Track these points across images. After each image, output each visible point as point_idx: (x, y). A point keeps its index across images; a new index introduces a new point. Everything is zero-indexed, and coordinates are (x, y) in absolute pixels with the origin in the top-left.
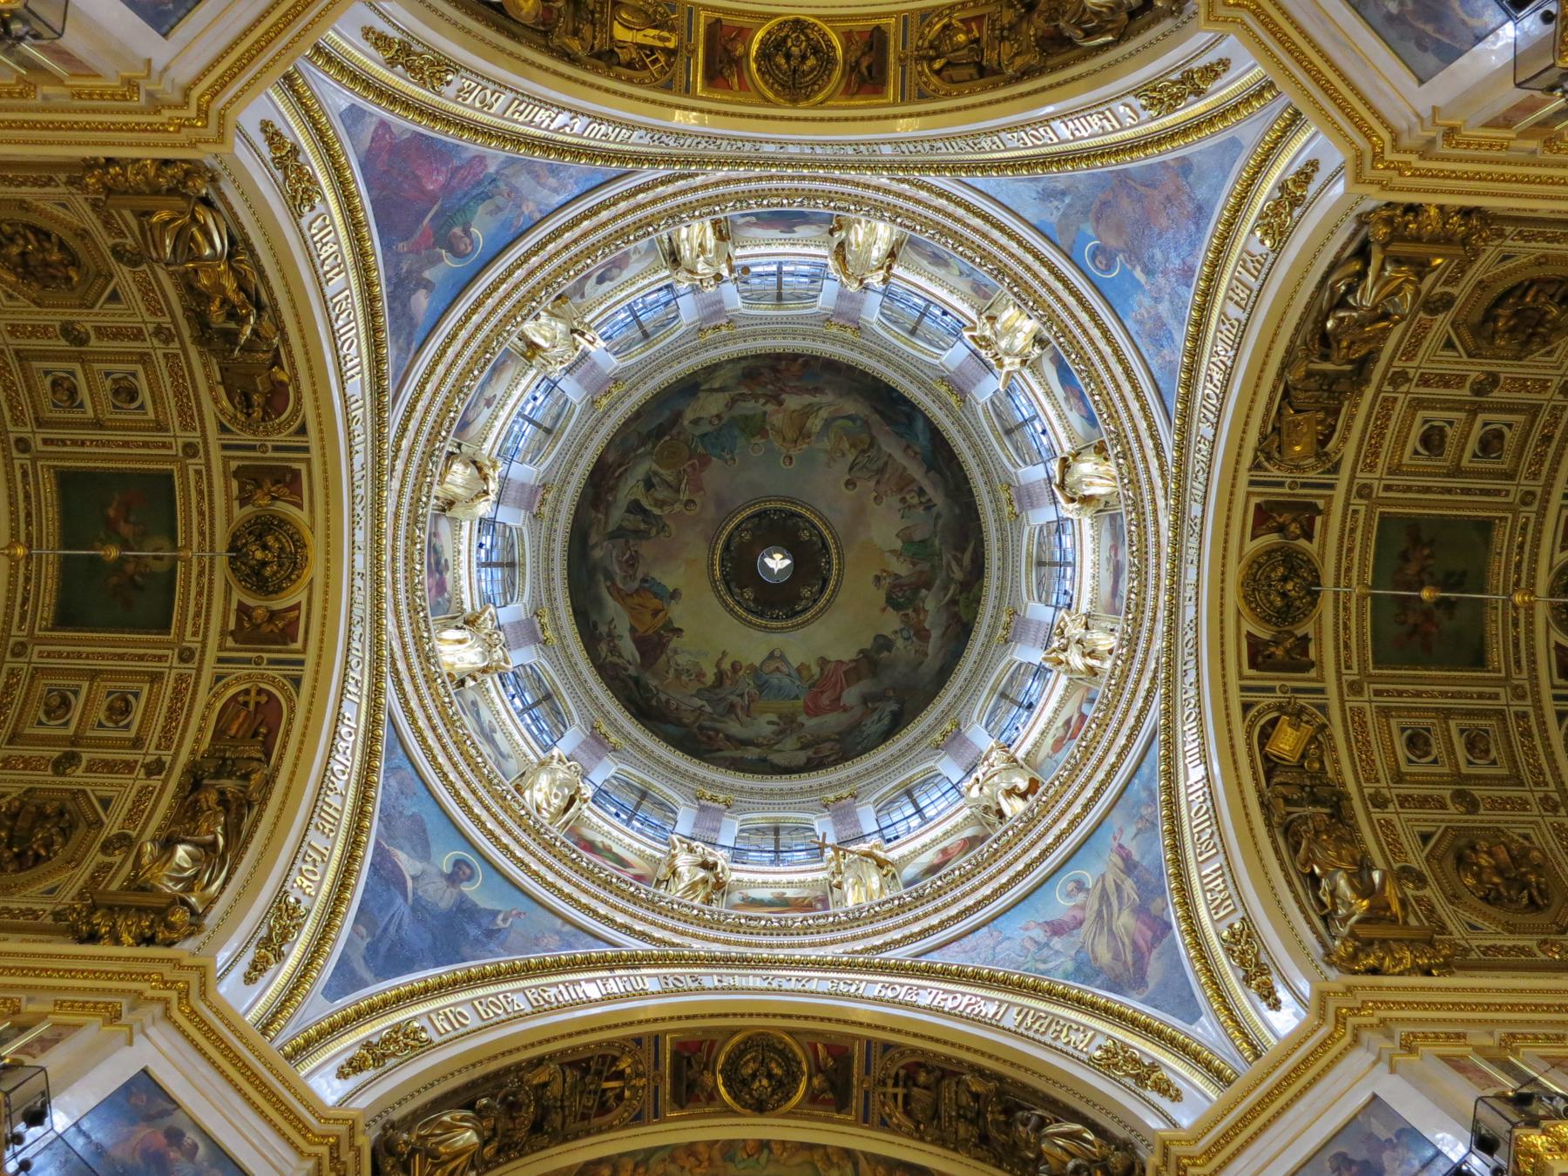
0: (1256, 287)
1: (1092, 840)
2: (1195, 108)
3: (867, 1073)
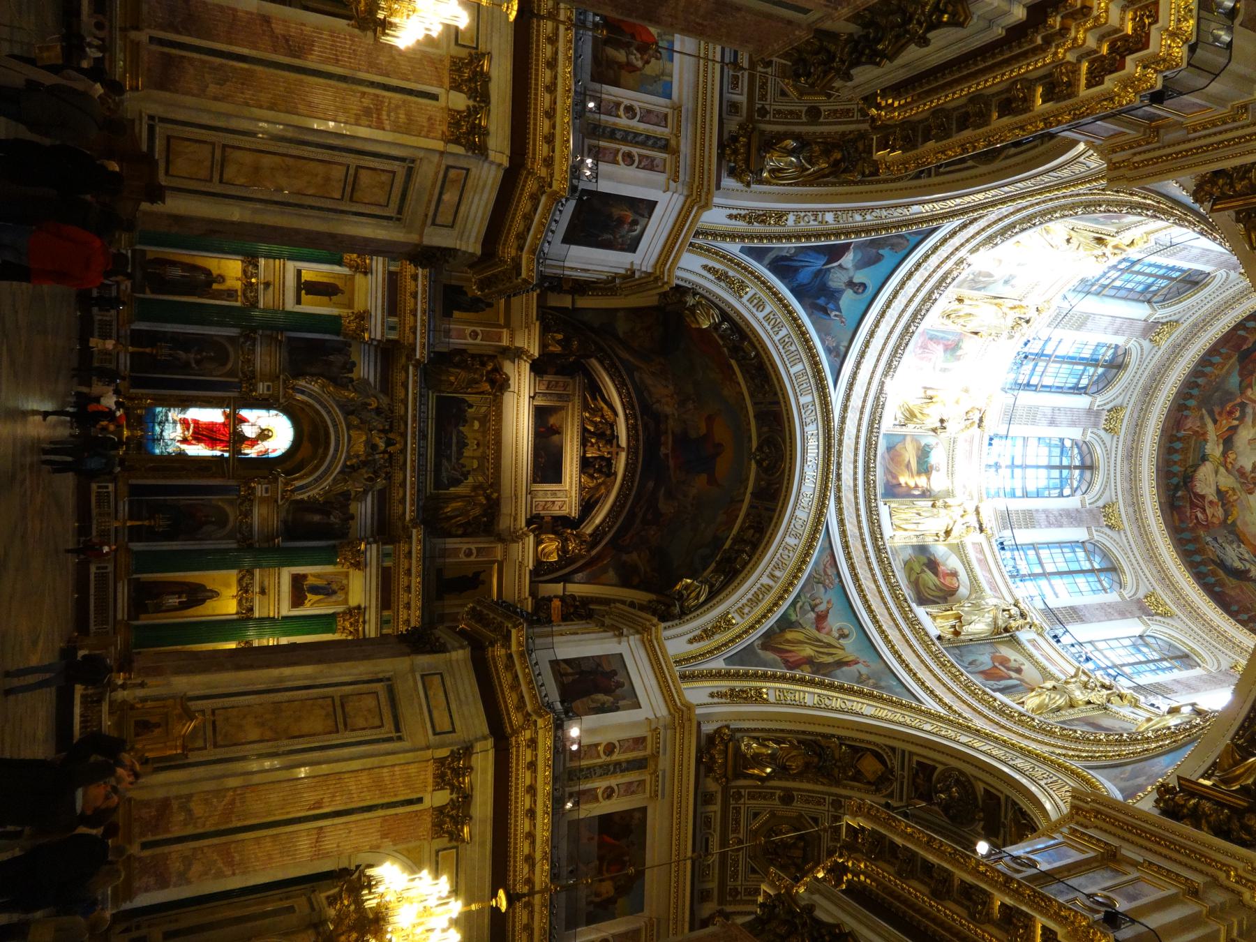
3: (767, 509)
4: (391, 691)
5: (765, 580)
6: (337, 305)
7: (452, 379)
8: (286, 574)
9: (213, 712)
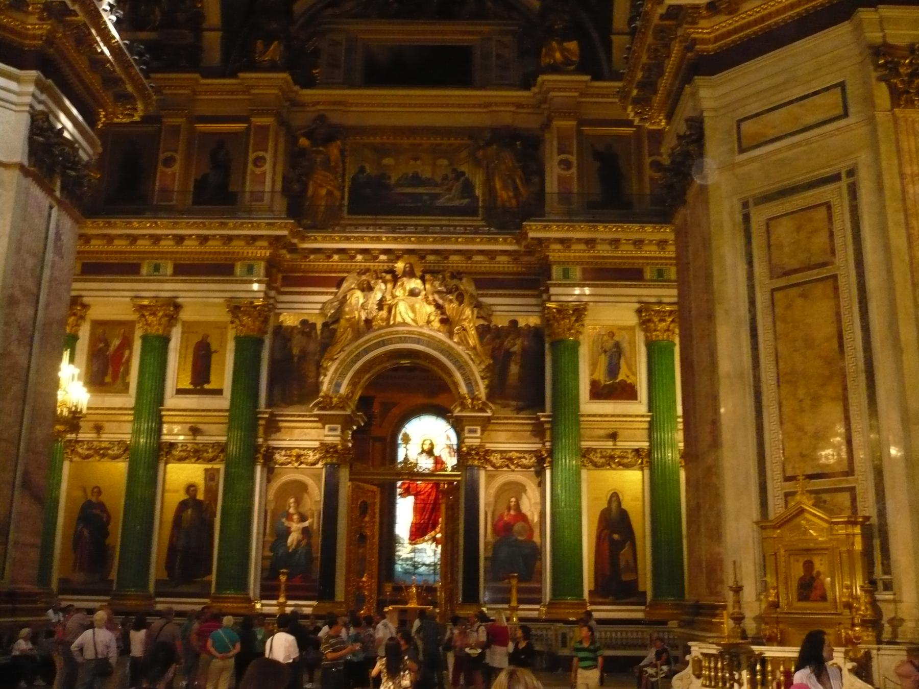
4: (766, 198)
6: (223, 344)
7: (323, 192)
8: (589, 407)
9: (788, 479)
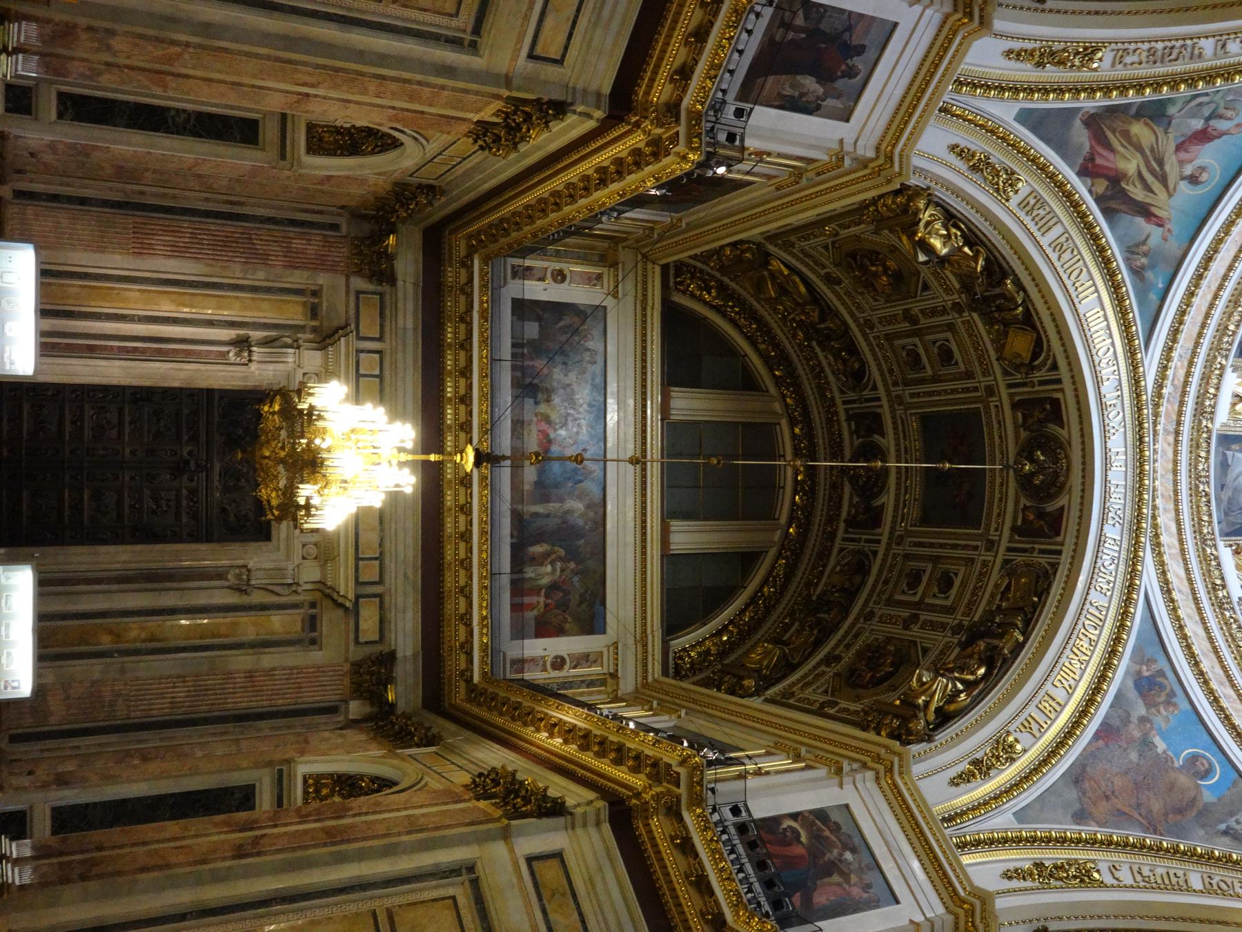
0: (1031, 710)
1: (1196, 224)
2: (1051, 856)
5: (1208, 45)
